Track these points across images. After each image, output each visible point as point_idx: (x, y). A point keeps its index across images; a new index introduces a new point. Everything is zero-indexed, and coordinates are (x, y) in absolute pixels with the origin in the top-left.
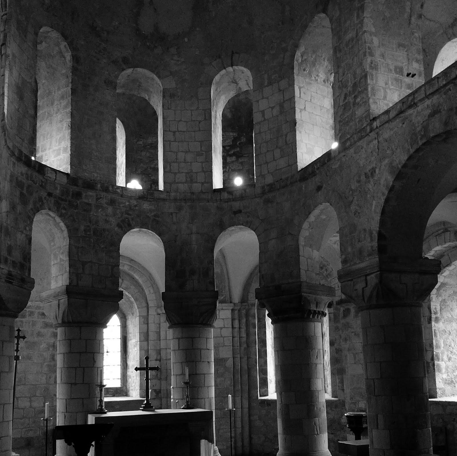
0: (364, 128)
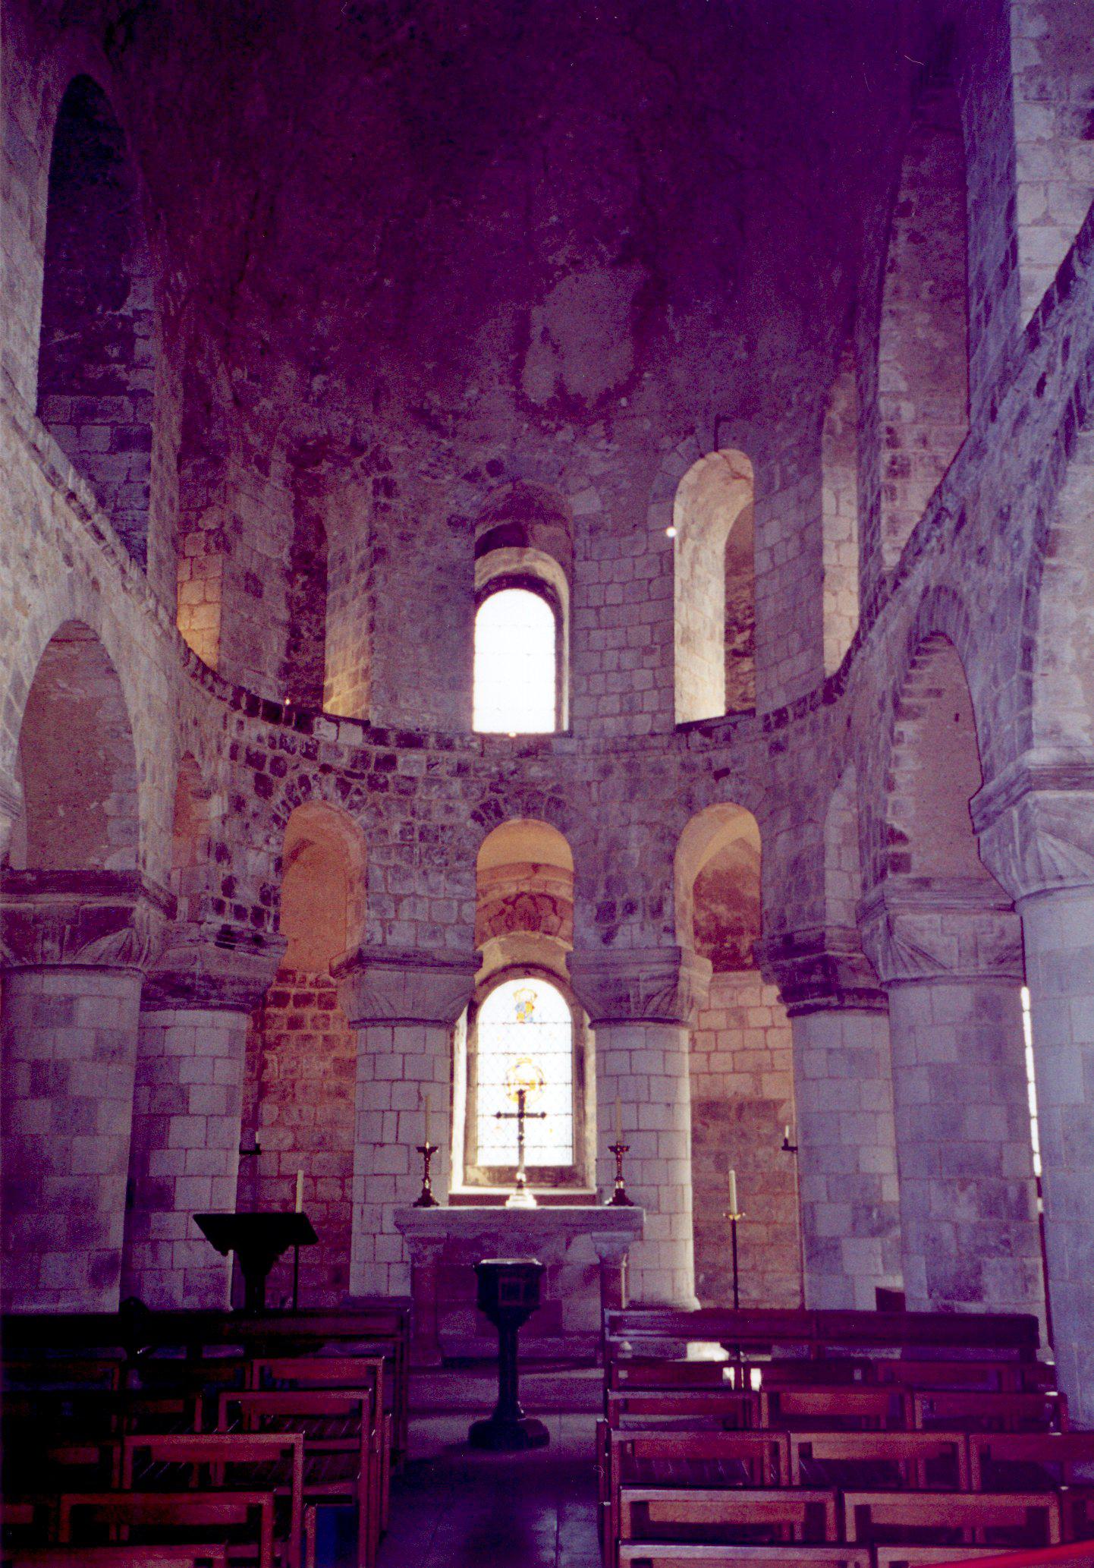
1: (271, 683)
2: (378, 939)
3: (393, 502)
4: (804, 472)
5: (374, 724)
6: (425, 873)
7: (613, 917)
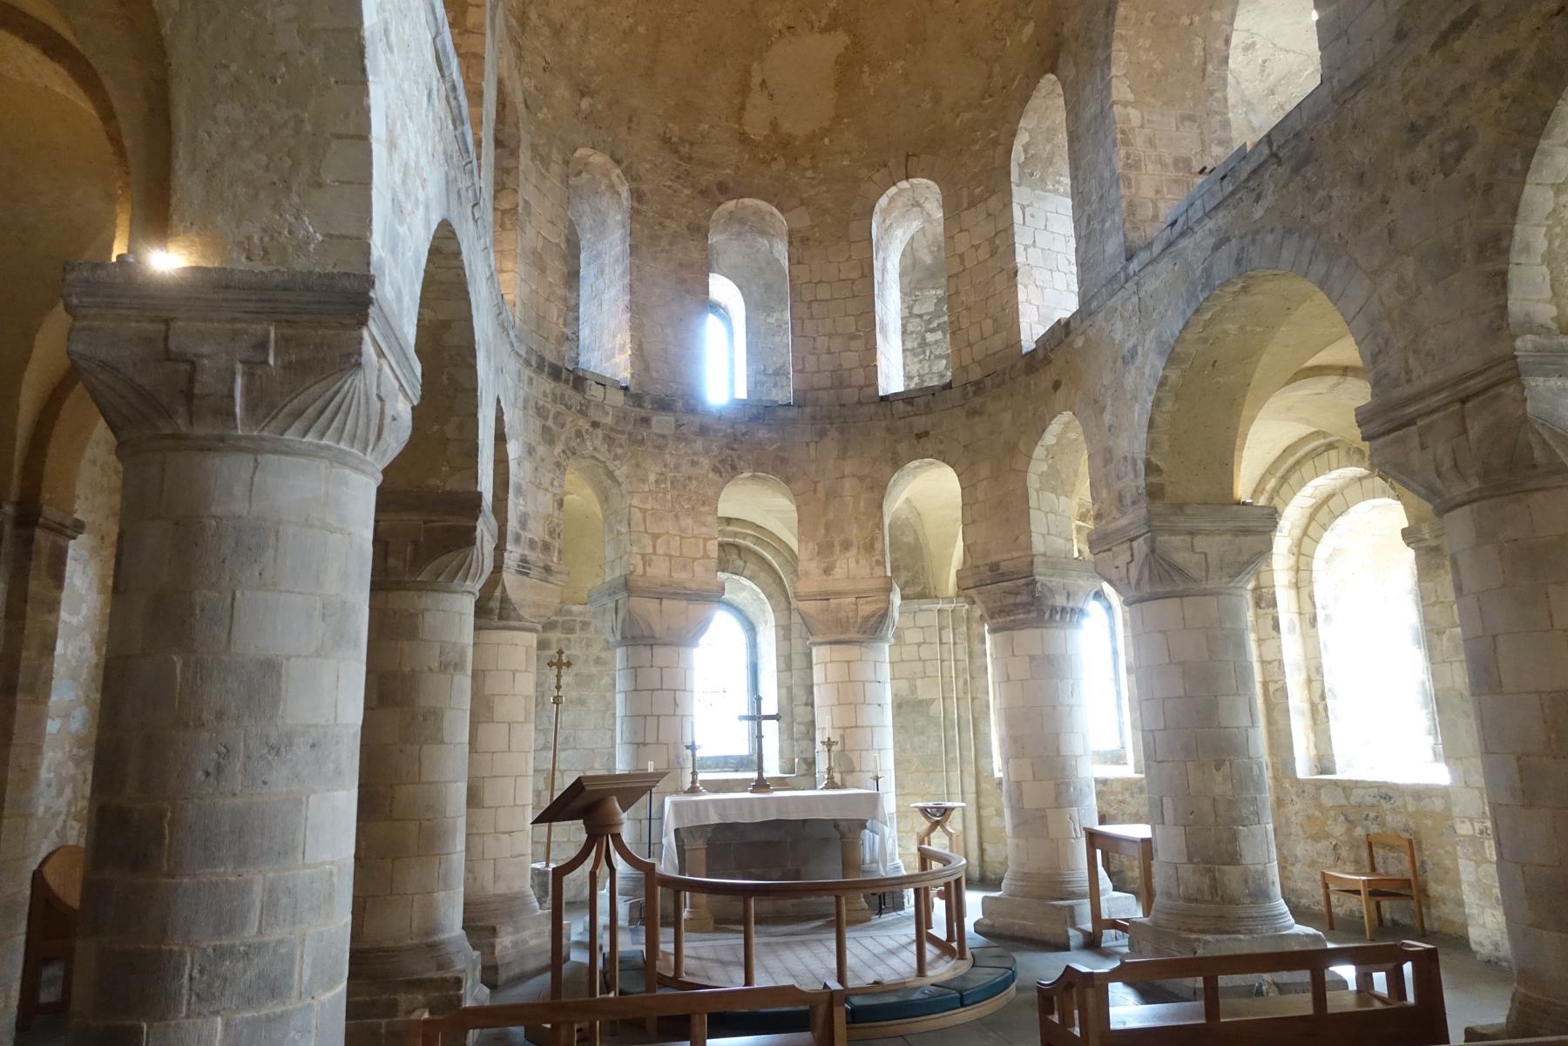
0: (1116, 276)
1: (553, 347)
2: (640, 570)
3: (644, 208)
4: (993, 192)
5: (632, 389)
6: (676, 516)
7: (832, 553)
